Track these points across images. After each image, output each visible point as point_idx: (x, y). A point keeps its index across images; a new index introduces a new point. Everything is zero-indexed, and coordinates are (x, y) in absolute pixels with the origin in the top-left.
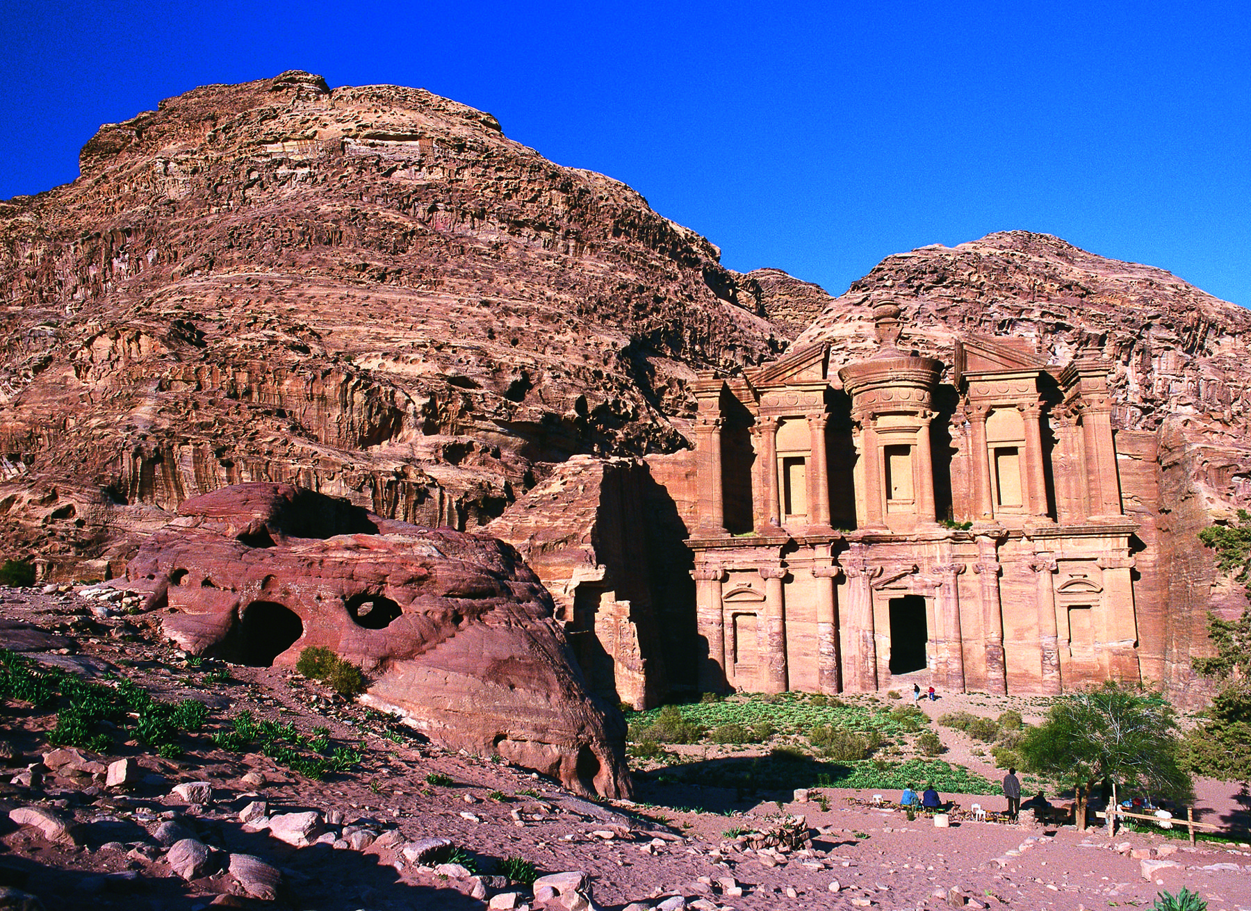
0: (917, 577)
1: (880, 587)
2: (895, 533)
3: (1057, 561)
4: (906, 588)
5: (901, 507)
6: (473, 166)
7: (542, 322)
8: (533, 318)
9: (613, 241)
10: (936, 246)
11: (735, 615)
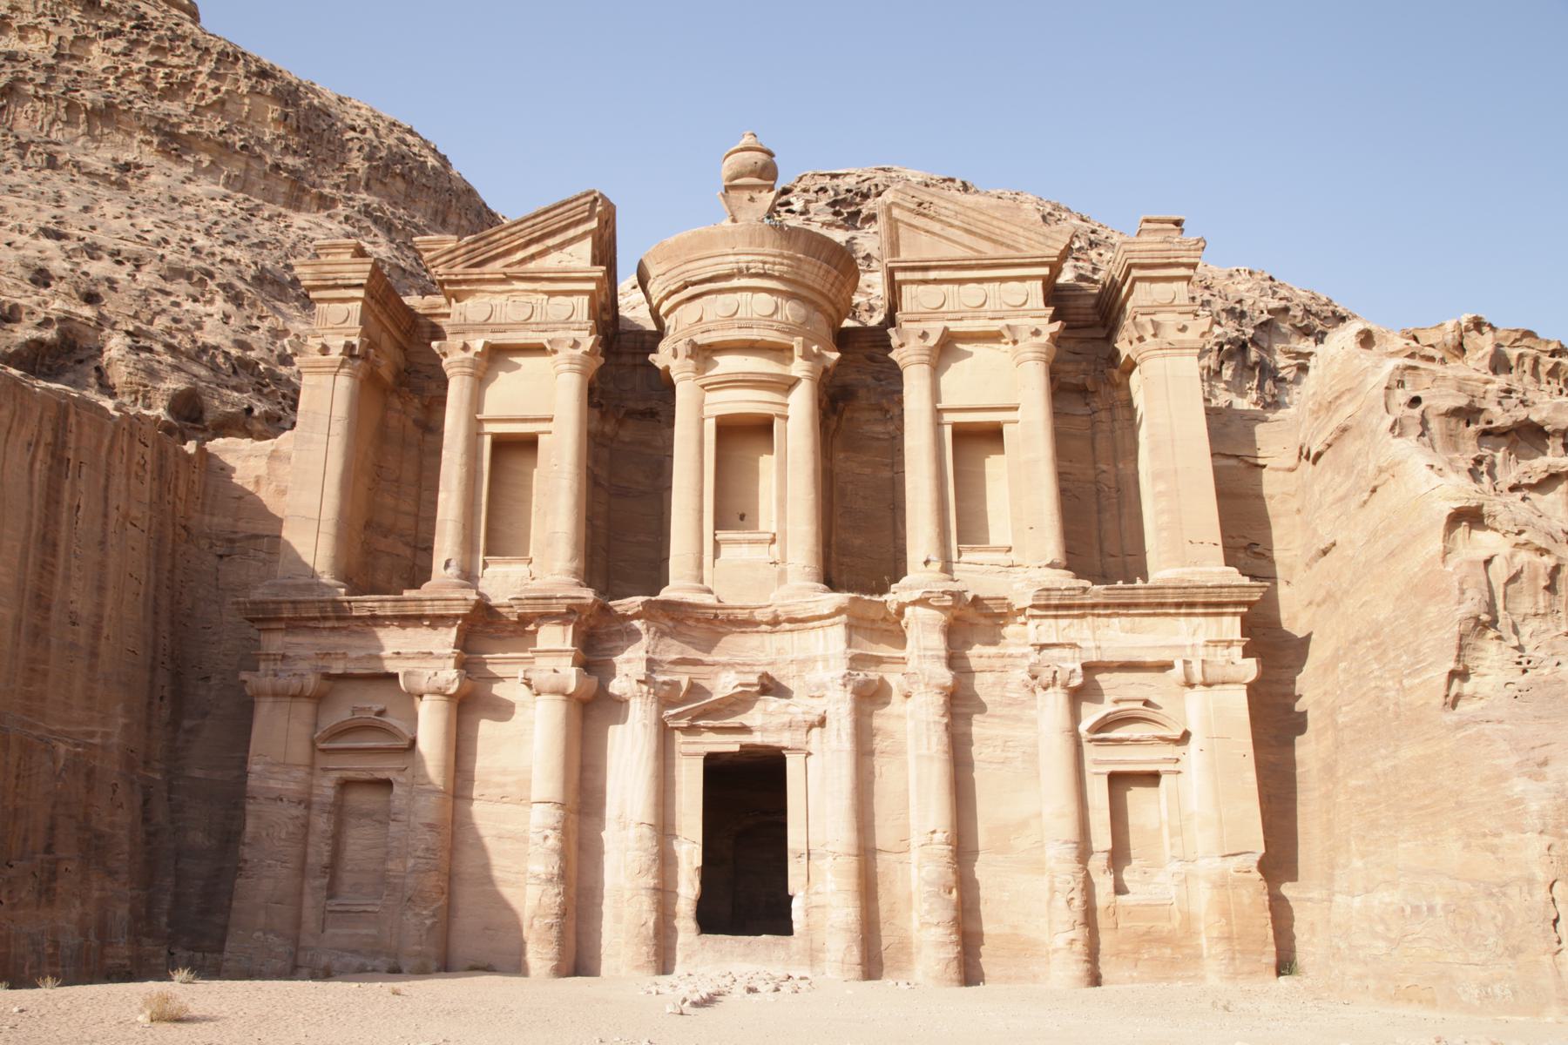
0: (772, 703)
1: (684, 723)
2: (728, 602)
3: (1089, 668)
5: (745, 548)
6: (108, 36)
7: (164, 278)
8: (146, 269)
9: (364, 196)
10: (895, 168)
11: (345, 785)
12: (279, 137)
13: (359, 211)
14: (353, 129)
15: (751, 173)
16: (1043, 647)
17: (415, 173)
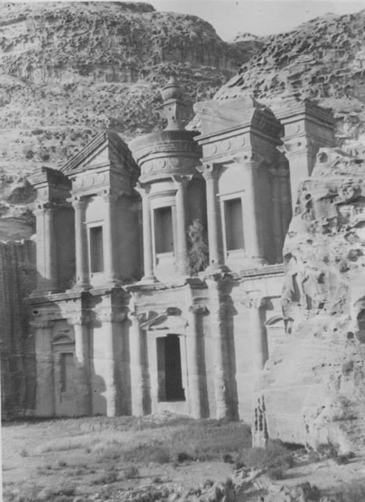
4: (166, 328)
7: (73, 140)
12: (124, 50)
13: (160, 73)
14: (155, 33)
15: (170, 98)
16: (248, 293)
17: (184, 44)
